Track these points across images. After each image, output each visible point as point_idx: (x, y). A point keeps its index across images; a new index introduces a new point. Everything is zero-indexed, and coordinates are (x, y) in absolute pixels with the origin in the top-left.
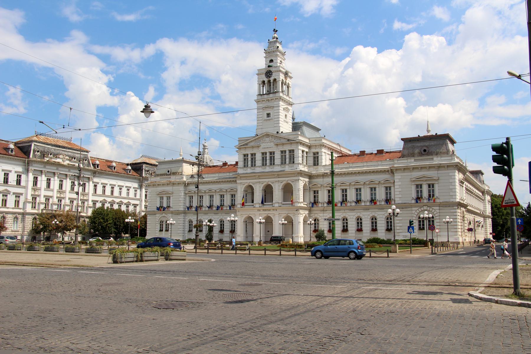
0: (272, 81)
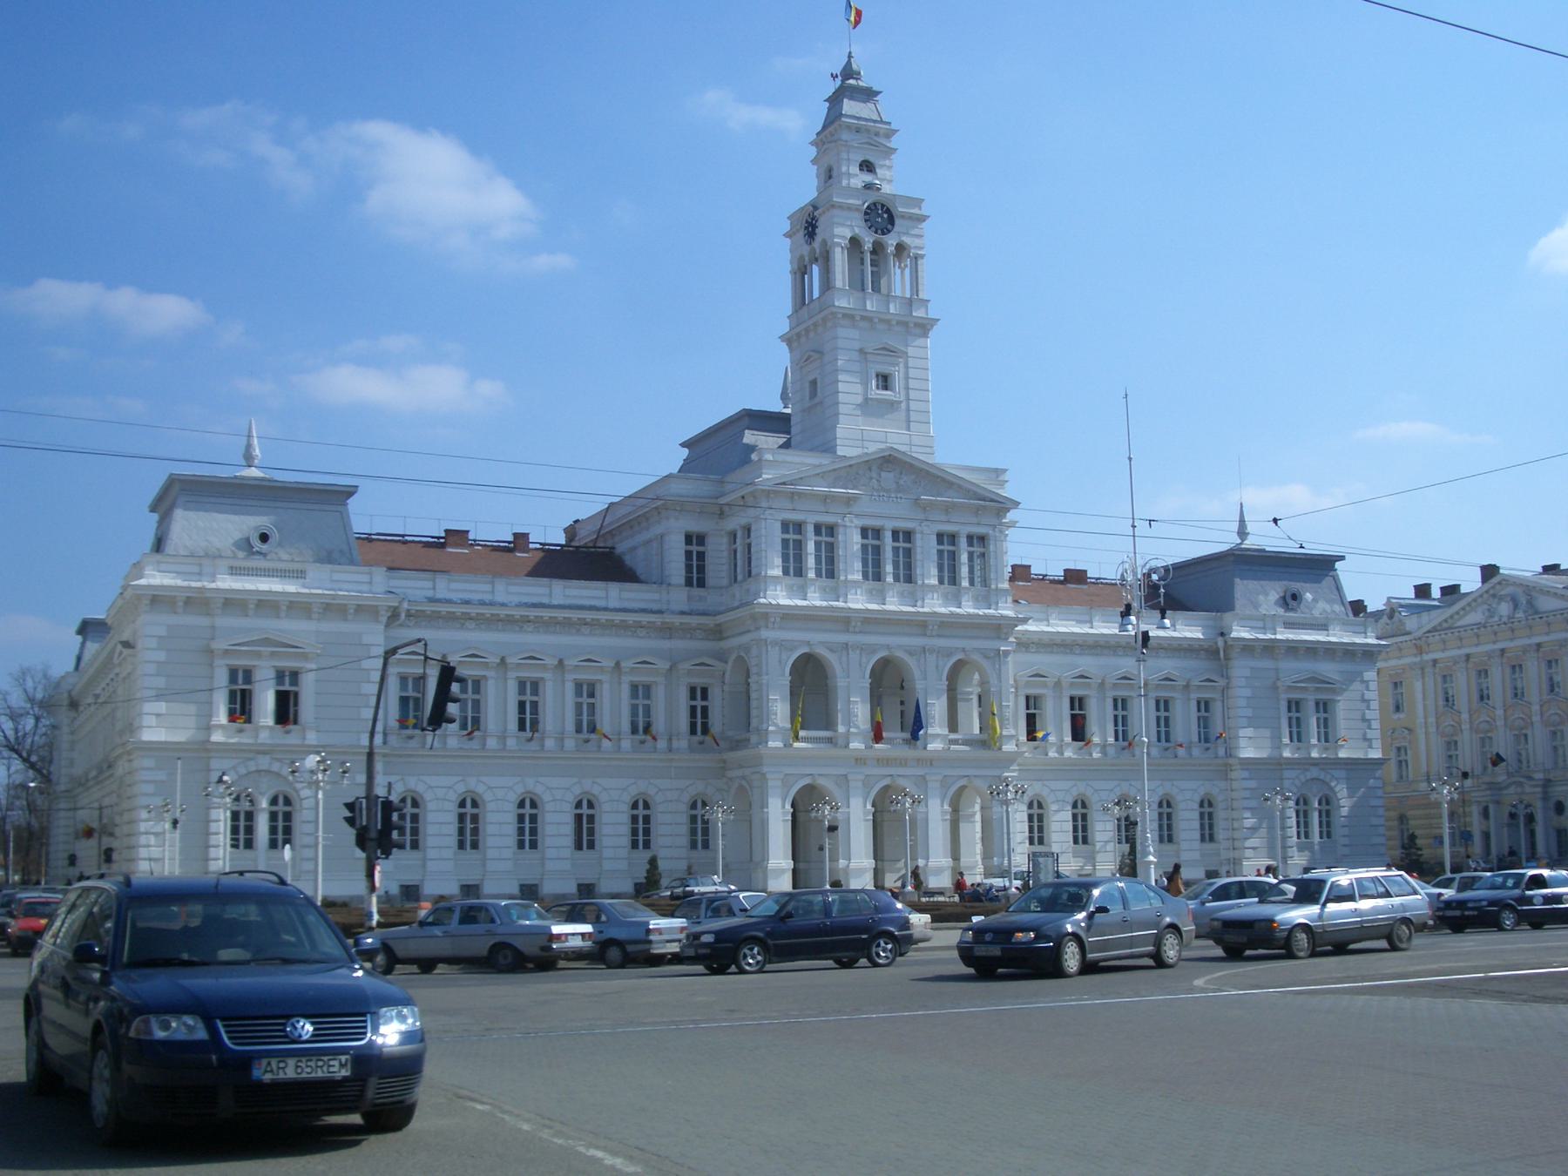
0: (891, 249)
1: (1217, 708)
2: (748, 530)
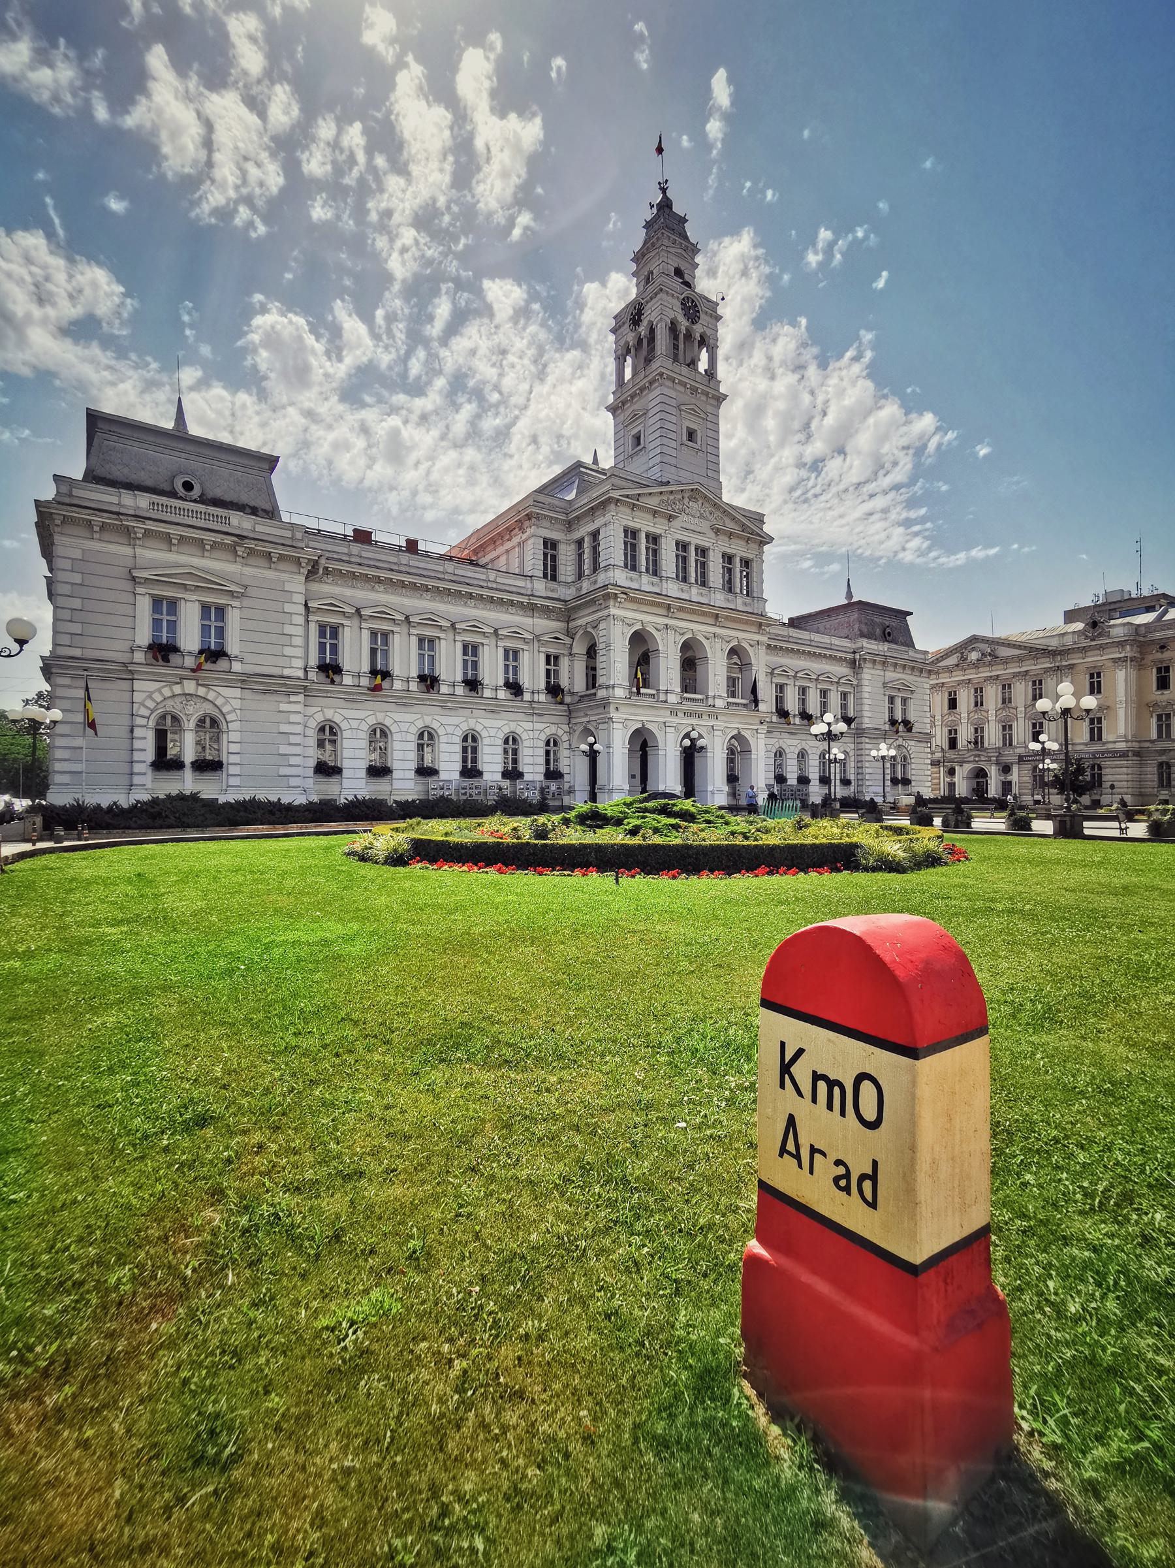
1: (851, 698)
2: (595, 535)
